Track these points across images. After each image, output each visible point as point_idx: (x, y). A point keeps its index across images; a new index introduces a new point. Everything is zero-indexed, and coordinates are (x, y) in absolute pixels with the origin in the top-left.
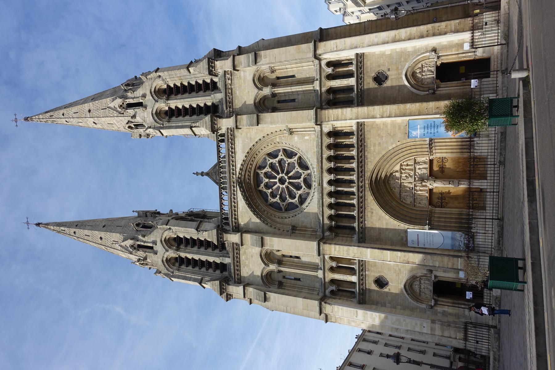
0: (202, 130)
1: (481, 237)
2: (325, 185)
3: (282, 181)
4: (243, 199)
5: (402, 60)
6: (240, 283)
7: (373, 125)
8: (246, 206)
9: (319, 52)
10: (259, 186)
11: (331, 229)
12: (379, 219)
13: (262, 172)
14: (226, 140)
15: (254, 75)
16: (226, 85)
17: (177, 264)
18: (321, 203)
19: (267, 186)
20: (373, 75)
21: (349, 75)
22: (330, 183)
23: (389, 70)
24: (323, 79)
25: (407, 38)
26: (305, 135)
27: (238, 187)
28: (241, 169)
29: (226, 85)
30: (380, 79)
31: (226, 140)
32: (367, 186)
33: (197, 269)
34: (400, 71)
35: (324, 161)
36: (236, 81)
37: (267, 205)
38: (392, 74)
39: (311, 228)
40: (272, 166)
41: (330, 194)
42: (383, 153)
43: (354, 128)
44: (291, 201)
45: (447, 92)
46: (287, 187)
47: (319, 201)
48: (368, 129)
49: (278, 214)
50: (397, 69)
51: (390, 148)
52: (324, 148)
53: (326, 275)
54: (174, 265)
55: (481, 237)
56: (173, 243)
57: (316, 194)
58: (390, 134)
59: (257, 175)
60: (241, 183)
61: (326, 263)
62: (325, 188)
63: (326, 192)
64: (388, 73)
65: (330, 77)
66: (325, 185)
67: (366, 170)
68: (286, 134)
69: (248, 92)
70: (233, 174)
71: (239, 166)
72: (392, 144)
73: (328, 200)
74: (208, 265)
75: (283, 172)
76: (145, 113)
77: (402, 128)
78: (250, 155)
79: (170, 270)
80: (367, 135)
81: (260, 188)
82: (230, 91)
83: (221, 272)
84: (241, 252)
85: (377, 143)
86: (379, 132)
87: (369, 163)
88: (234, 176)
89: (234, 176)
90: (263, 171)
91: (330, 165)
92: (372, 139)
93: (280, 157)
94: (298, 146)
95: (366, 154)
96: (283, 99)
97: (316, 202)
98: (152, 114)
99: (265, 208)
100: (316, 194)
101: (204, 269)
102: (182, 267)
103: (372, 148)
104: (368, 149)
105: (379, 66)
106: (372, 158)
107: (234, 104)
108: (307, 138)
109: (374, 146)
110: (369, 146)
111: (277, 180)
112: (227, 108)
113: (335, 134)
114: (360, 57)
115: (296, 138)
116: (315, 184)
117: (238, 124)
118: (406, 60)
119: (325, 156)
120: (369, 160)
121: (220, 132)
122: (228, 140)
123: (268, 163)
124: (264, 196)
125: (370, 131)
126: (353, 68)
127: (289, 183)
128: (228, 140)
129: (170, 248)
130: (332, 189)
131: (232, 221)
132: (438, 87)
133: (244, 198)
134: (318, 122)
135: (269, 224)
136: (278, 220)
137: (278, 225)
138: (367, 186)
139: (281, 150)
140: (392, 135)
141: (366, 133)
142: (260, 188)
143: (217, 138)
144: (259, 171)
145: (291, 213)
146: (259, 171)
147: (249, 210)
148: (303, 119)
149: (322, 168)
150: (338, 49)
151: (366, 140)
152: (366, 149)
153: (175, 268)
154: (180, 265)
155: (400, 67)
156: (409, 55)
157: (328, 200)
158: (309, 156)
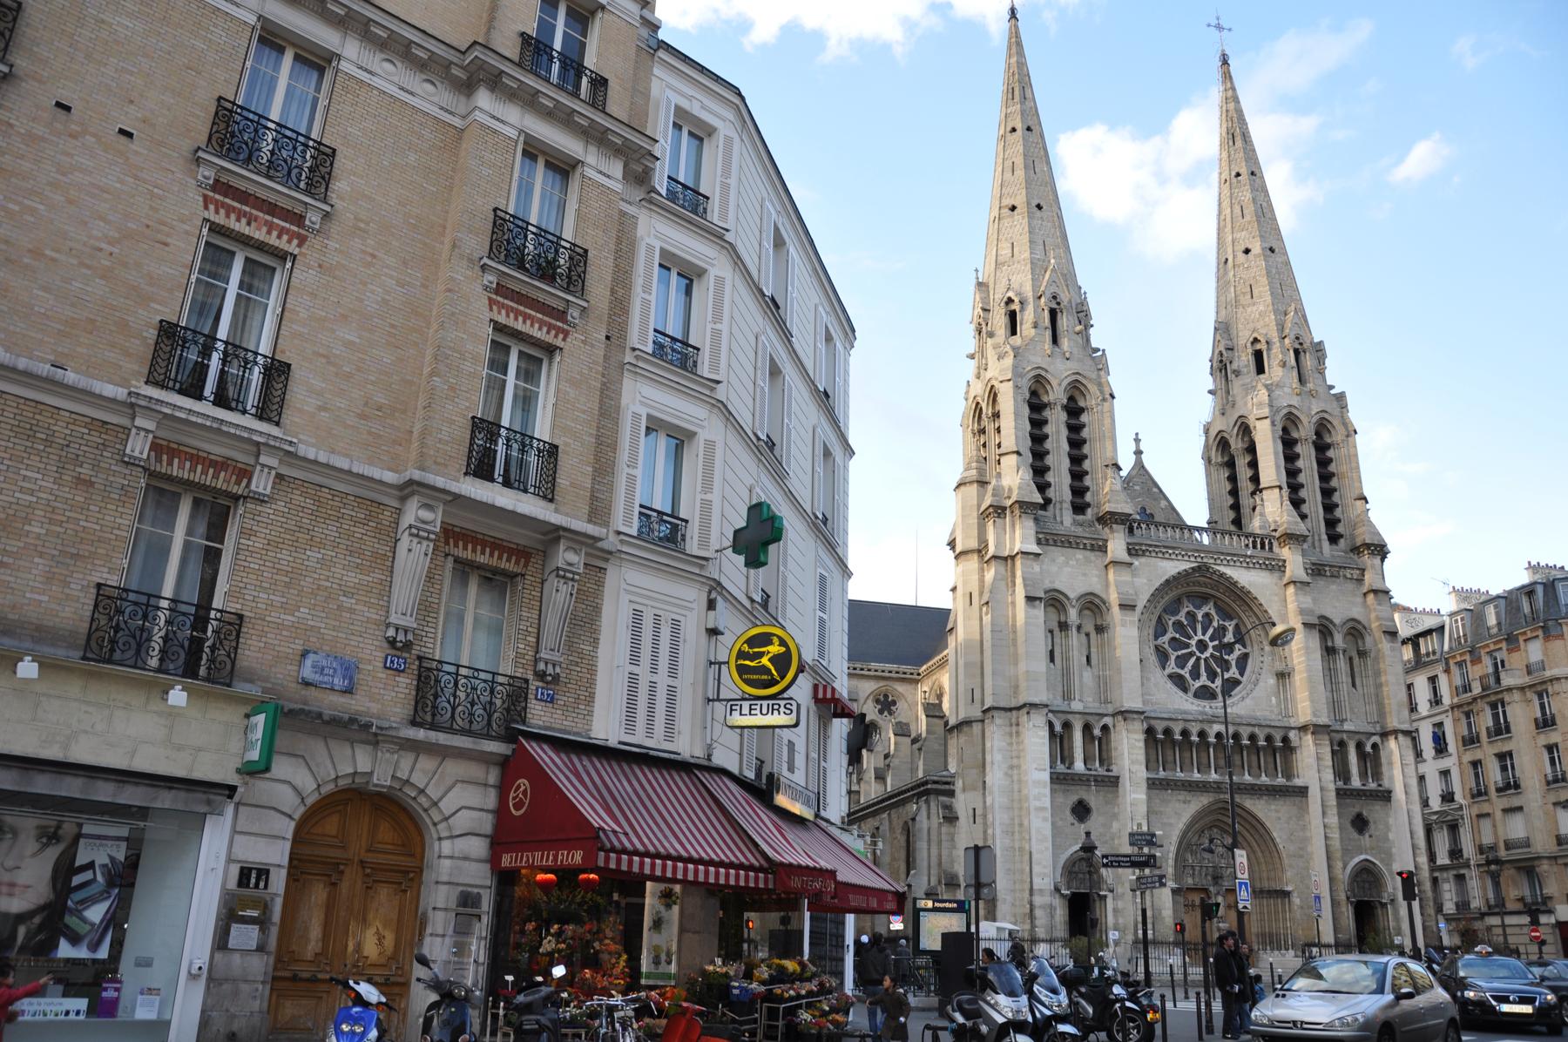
3: (1202, 646)
7: (1304, 809)
9: (1400, 737)
13: (1209, 608)
19: (1191, 616)
21: (1363, 775)
26: (1278, 697)
28: (1222, 575)
30: (1360, 824)
36: (1350, 586)
38: (1366, 840)
42: (1268, 824)
43: (1298, 782)
46: (1191, 654)
47: (1185, 712)
51: (1275, 835)
52: (1267, 730)
60: (1202, 569)
63: (1206, 727)
68: (1279, 667)
71: (1228, 571)
73: (1194, 729)
78: (1242, 597)
80: (1289, 801)
81: (1186, 602)
90: (1213, 612)
94: (1261, 684)
113: (1288, 748)
114: (1385, 796)
115: (1272, 681)
116: (1206, 707)
121: (1275, 544)
124: (1173, 608)
126: (1372, 785)
127: (1198, 659)
134: (1317, 730)
142: (1186, 602)
148: (1306, 703)
157: (1194, 729)
158: (1248, 701)
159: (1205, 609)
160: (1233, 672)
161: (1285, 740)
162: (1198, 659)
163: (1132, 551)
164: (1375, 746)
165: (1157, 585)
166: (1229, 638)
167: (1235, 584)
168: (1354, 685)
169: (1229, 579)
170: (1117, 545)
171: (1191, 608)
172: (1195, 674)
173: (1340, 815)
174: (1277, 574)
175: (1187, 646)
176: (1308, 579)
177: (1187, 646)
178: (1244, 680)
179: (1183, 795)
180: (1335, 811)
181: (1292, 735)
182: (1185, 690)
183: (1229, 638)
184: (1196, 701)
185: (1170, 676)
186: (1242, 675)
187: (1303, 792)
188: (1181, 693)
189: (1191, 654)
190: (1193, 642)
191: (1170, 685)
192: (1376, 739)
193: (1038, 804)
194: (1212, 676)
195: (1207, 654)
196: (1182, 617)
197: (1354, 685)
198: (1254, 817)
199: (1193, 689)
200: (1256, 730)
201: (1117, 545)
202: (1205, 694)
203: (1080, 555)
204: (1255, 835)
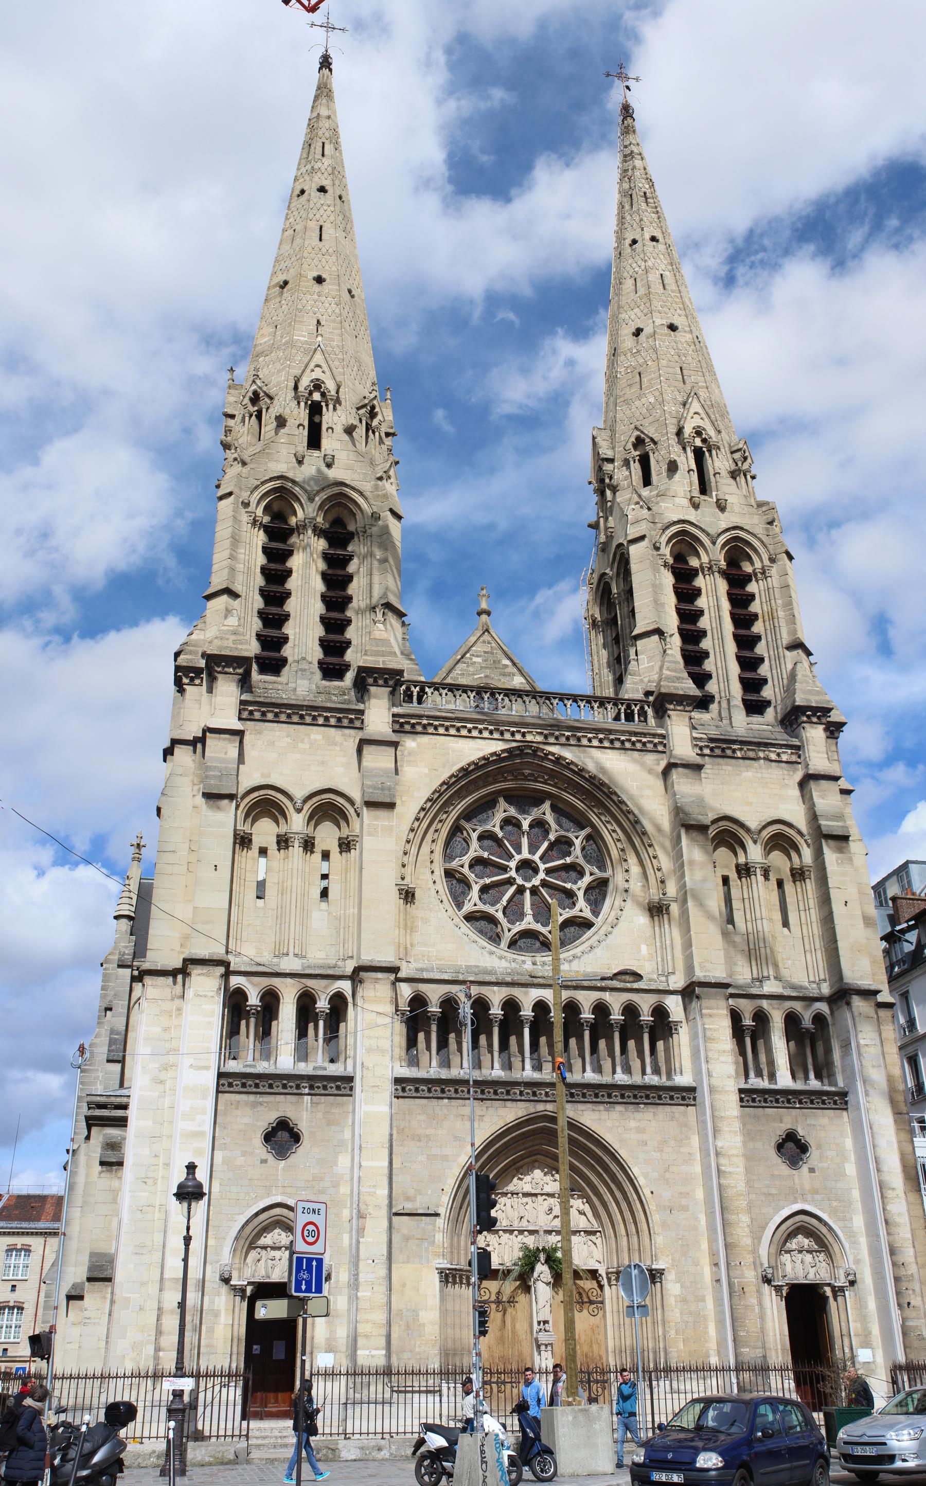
0: (650, 659)
1: (430, 1406)
2: (535, 994)
3: (527, 866)
4: (481, 755)
5: (835, 1204)
6: (240, 719)
8: (463, 763)
10: (510, 800)
11: (418, 1001)
12: (456, 1138)
13: (546, 811)
14: (631, 727)
15: (790, 825)
16: (767, 745)
17: (266, 519)
18: (488, 978)
20: (801, 1132)
22: (541, 1007)
23: (812, 1170)
24: (788, 1004)
25: (888, 1217)
27: (514, 744)
28: (559, 760)
29: (767, 745)
30: (793, 1148)
31: (631, 727)
32: (540, 1107)
33: (260, 581)
34: (809, 1197)
35: (595, 995)
36: (776, 772)
37: (458, 819)
39: (412, 945)
40: (562, 845)
41: (511, 1006)
42: (624, 1153)
44: (476, 888)
45: (769, 1312)
46: (510, 882)
48: (677, 1115)
49: (439, 847)
50: (815, 1192)
51: (636, 1171)
53: (289, 980)
54: (267, 509)
55: (430, 1406)
56: (330, 517)
57: (504, 964)
58: (667, 1170)
59: (537, 799)
61: (323, 982)
62: (526, 994)
64: (805, 1169)
65: (791, 1020)
66: (535, 994)
67: (580, 1106)
69: (750, 804)
70: (546, 737)
71: (568, 754)
72: (646, 1176)
73: (496, 997)
74: (273, 616)
75: (548, 871)
76: (686, 502)
77: (684, 1202)
79: (257, 495)
80: (663, 1112)
82: (751, 754)
83: (257, 658)
84: (333, 730)
85: (645, 1137)
86: (672, 1143)
87: (596, 1115)
88: (540, 739)
89: (540, 739)
90: (550, 818)
91: (587, 1009)
92: (654, 1124)
93: (588, 868)
94: (622, 924)
95: (619, 1108)
96: (735, 893)
97: (482, 964)
98: (684, 522)
99: (454, 815)
100: (504, 964)
101: (259, 603)
102: (261, 532)
103: (633, 1124)
104: (630, 1114)
105: (819, 1147)
106: (609, 1124)
107: (720, 760)
108: (644, 949)
109: (640, 1130)
110: (639, 1116)
111: (536, 858)
112: (712, 740)
113: (662, 1026)
115: (642, 920)
117: (680, 770)
118: (833, 1212)
119: (607, 996)
120: (604, 1115)
122: (636, 734)
123: (571, 835)
125: (673, 1118)
128: (636, 734)
129: (320, 508)
130: (527, 1012)
131: (420, 717)
132: (778, 1289)
133: (484, 758)
135: (417, 824)
136: (426, 849)
137: (414, 851)
138: (540, 1107)
139: (604, 875)
140: (667, 1175)
141: (668, 1108)
142: (502, 803)
143: (636, 702)
144: (547, 806)
145: (442, 885)
146: (547, 806)
147: (455, 769)
149: (576, 988)
150: (862, 1050)
151: (651, 1109)
152: (631, 1107)
153: (260, 511)
154: (267, 529)
155: (818, 1197)
156: (844, 1219)
157: (496, 997)
158: (598, 952)
159: (535, 813)
160: (582, 908)
161: (660, 1012)
162: (521, 890)
163: (404, 726)
164: (819, 1019)
165: (445, 776)
166: (576, 855)
167: (581, 772)
168: (786, 924)
169: (569, 765)
170: (379, 714)
171: (512, 811)
172: (514, 911)
173: (749, 1135)
174: (650, 758)
175: (505, 869)
176: (699, 760)
177: (505, 869)
178: (598, 921)
179: (465, 1108)
180: (737, 1125)
181: (674, 1005)
182: (496, 939)
183: (576, 855)
184: (510, 955)
185: (469, 918)
186: (596, 913)
187: (686, 1095)
188: (483, 942)
189: (510, 882)
190: (513, 864)
191: (466, 928)
192: (823, 1007)
193: (190, 1126)
194: (543, 913)
195: (536, 881)
196: (494, 824)
197: (786, 924)
198: (598, 1142)
199: (507, 937)
200: (607, 996)
201: (379, 714)
202: (528, 940)
203: (317, 734)
204: (596, 1172)
